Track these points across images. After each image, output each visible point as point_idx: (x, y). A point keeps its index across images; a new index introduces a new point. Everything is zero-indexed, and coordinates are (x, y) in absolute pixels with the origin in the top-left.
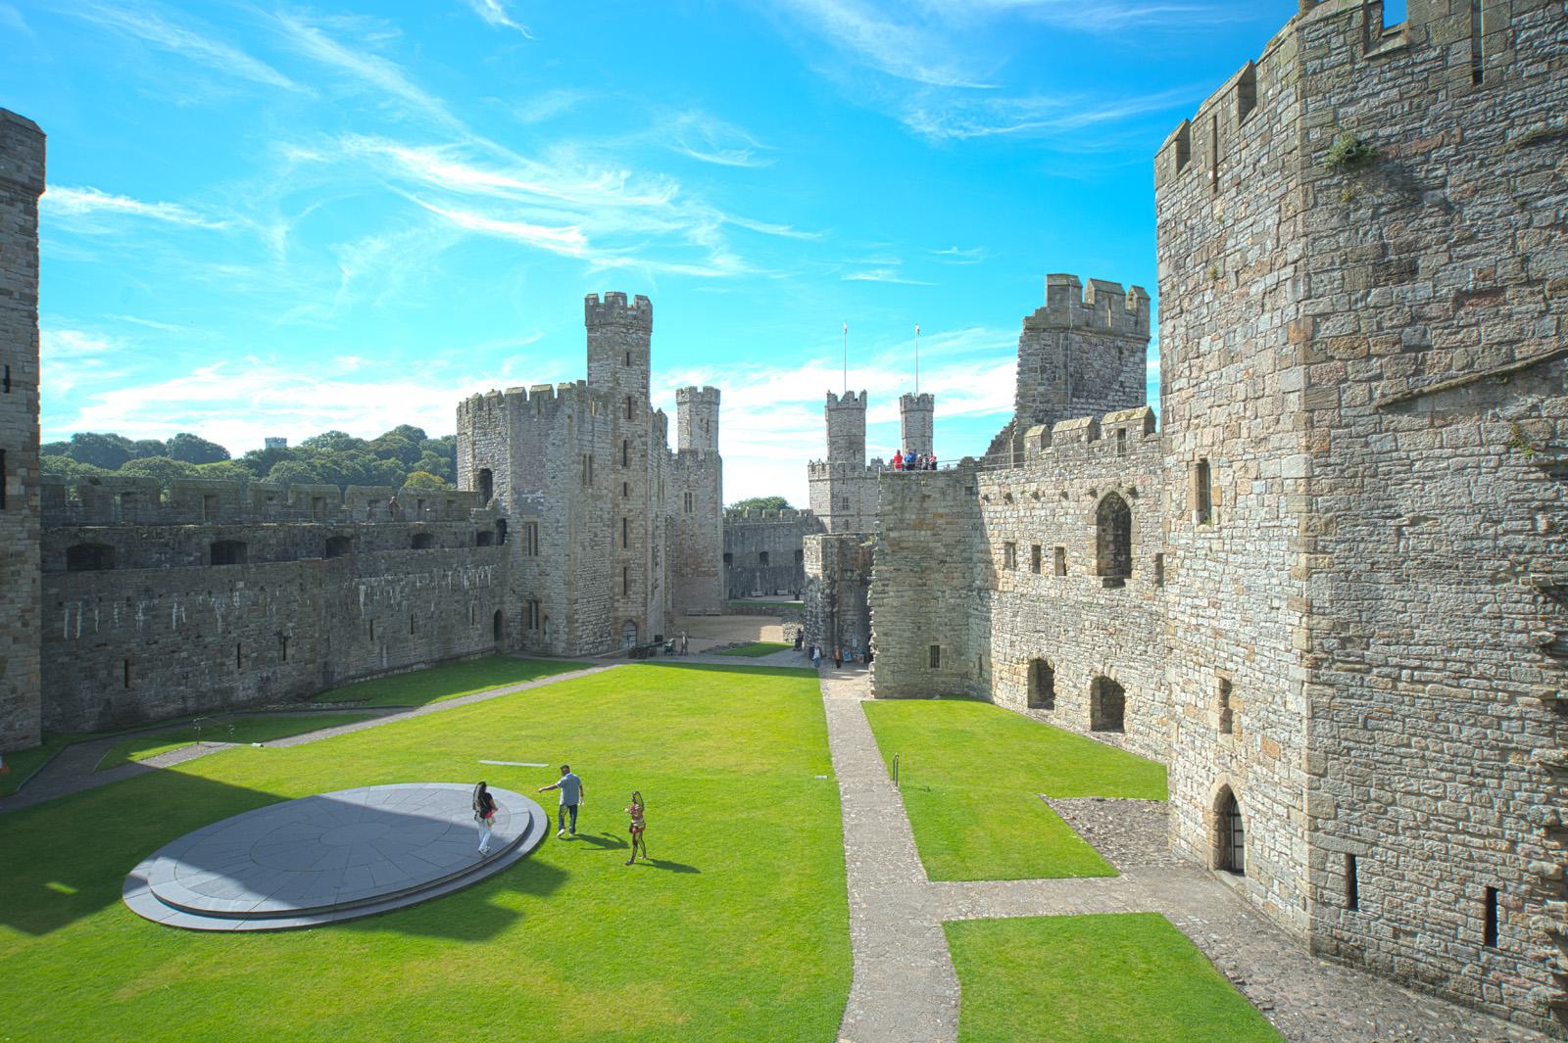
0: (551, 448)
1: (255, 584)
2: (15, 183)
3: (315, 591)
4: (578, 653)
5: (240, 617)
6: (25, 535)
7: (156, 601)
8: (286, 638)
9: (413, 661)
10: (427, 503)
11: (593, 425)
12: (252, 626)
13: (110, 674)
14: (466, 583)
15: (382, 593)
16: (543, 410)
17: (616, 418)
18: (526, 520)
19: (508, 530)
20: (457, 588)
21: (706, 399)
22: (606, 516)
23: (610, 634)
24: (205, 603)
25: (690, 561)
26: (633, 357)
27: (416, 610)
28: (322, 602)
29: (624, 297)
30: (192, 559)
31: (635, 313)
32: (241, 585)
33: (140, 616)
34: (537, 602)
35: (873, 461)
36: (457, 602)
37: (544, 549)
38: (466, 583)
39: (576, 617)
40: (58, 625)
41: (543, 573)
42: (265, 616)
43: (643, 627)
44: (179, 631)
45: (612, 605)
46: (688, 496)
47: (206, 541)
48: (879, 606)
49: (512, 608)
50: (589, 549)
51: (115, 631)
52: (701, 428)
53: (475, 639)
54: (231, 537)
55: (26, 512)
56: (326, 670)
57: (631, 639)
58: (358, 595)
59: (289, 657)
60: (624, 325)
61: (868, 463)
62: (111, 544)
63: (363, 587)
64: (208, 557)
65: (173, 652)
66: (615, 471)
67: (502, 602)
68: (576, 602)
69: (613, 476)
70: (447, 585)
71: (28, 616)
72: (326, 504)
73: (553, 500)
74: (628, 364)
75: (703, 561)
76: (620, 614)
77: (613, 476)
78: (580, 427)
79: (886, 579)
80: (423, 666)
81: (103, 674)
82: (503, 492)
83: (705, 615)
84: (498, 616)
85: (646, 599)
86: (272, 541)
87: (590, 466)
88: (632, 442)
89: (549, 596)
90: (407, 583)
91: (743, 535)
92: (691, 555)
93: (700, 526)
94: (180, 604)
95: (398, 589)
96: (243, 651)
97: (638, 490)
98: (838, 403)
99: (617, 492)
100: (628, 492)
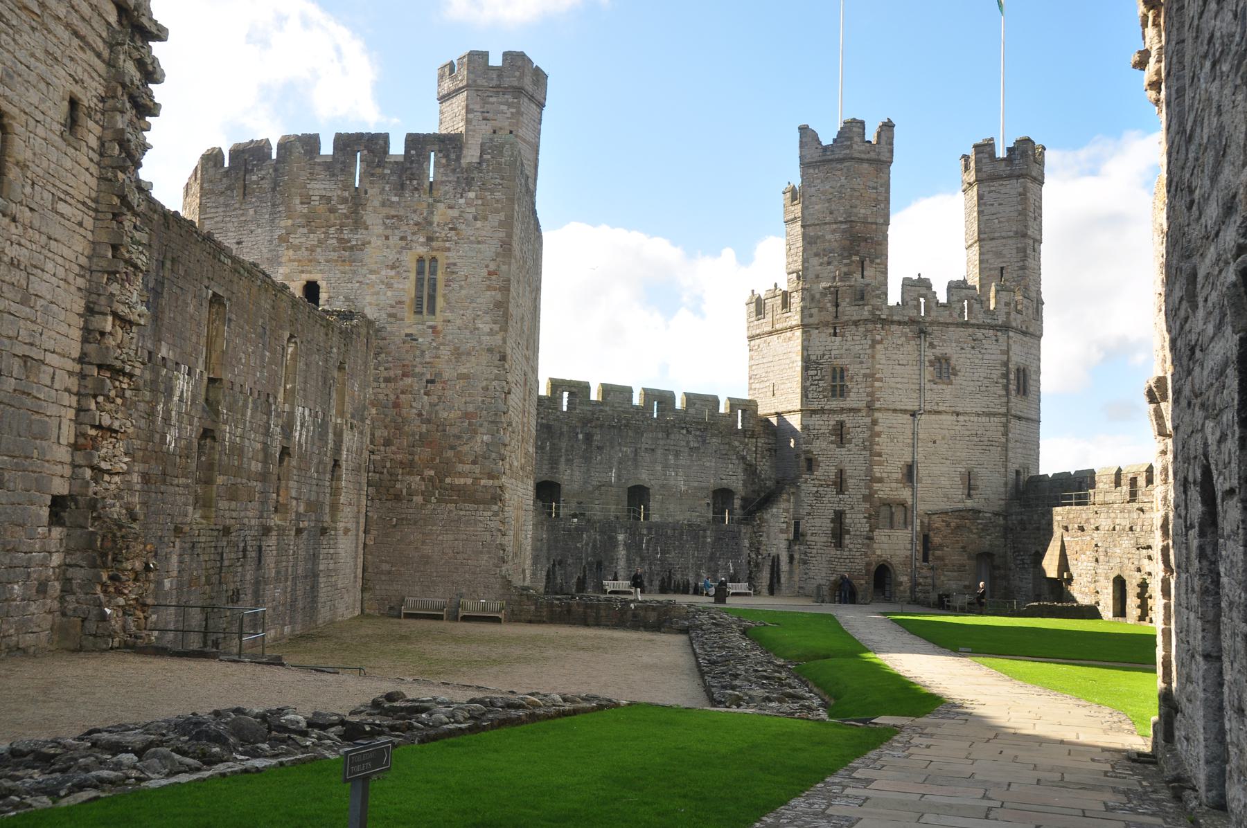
21: (507, 82)
25: (422, 454)
35: (907, 284)
61: (894, 296)
75: (458, 455)
83: (454, 618)
91: (588, 438)
92: (424, 440)
93: (458, 354)
98: (826, 148)
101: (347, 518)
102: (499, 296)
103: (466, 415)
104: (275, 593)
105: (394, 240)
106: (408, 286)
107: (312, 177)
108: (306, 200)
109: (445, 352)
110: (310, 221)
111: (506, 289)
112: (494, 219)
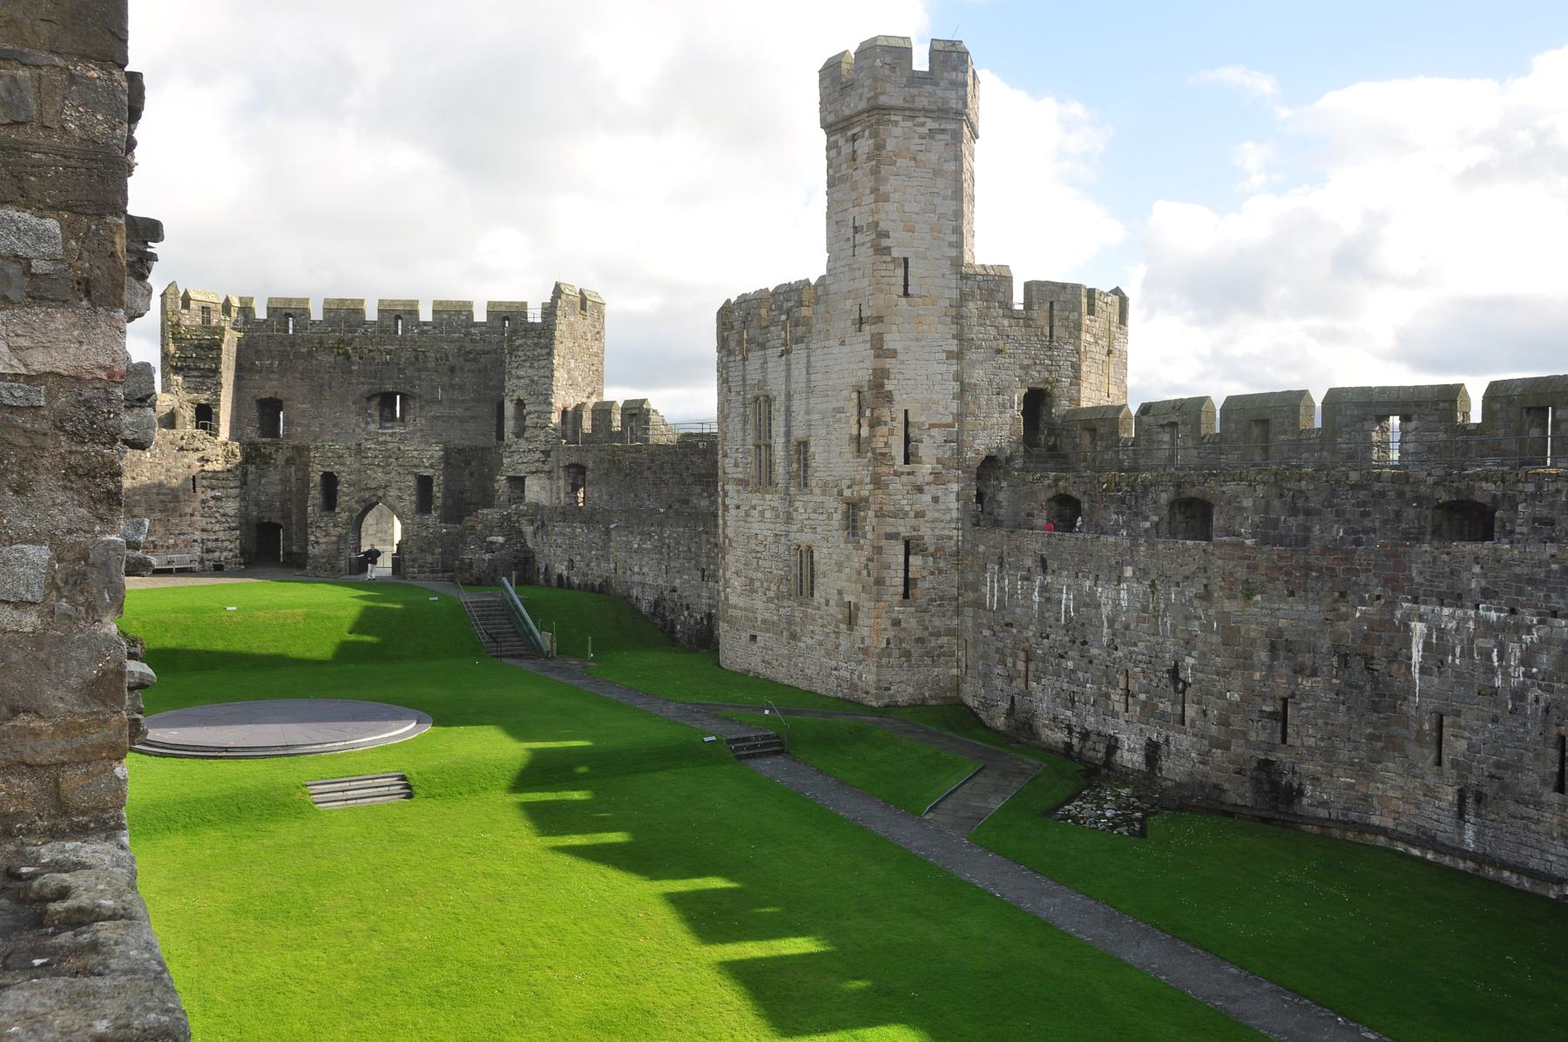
6: (868, 480)
7: (1049, 579)
15: (1467, 653)
24: (1092, 594)
30: (1148, 525)
32: (1128, 572)
33: (1036, 597)
44: (1067, 628)
47: (1164, 498)
51: (1018, 610)
58: (1409, 640)
63: (1418, 628)
64: (1164, 527)
65: (1061, 656)
71: (871, 565)
81: (1010, 660)
86: (1248, 503)
90: (1545, 642)
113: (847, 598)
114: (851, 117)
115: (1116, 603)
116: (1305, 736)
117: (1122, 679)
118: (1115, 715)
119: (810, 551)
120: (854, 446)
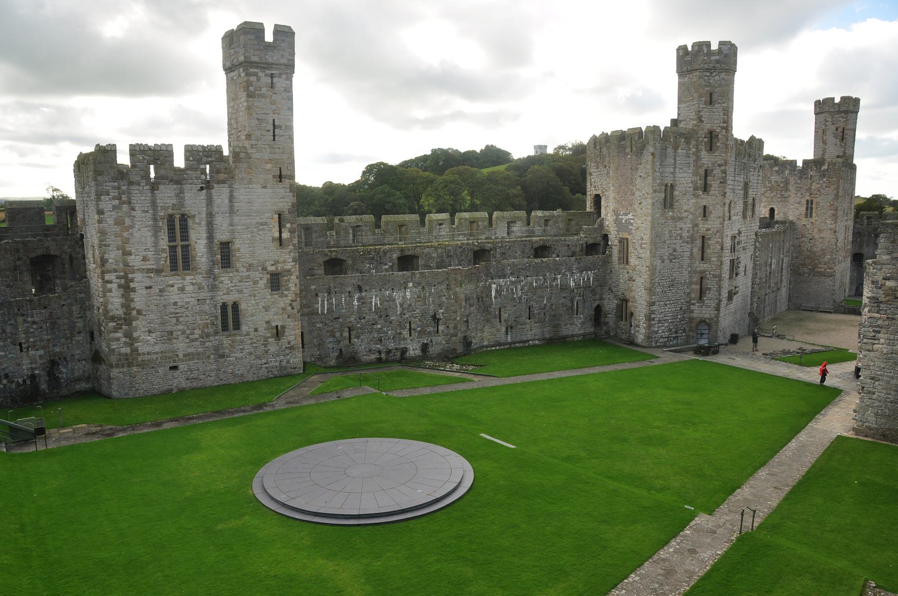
0: (639, 180)
1: (419, 284)
2: (281, 65)
3: (458, 289)
4: (654, 345)
5: (410, 305)
6: (291, 260)
7: (364, 294)
8: (439, 320)
9: (529, 338)
10: (551, 223)
11: (675, 159)
12: (418, 311)
13: (341, 335)
14: (572, 284)
15: (507, 290)
16: (634, 149)
17: (698, 151)
18: (621, 236)
19: (610, 243)
20: (564, 287)
22: (685, 234)
23: (684, 331)
25: (808, 261)
26: (715, 97)
27: (532, 303)
28: (462, 296)
29: (708, 44)
31: (718, 57)
32: (411, 285)
33: (356, 303)
34: (627, 301)
36: (564, 297)
37: (633, 260)
38: (572, 284)
39: (653, 316)
40: (316, 306)
41: (631, 279)
42: (425, 304)
43: (714, 327)
45: (689, 308)
46: (809, 203)
47: (395, 256)
48: (869, 351)
49: (610, 305)
50: (667, 262)
52: (836, 137)
53: (577, 326)
54: (409, 253)
55: (291, 247)
56: (467, 342)
57: (704, 336)
59: (440, 332)
60: (708, 70)
62: (345, 258)
63: (494, 286)
64: (396, 267)
66: (696, 196)
67: (601, 299)
68: (653, 304)
69: (694, 201)
70: (557, 285)
71: (294, 304)
72: (478, 226)
73: (639, 222)
74: (711, 103)
75: (820, 263)
76: (695, 315)
77: (694, 201)
78: (662, 162)
79: (878, 326)
80: (537, 342)
81: (338, 335)
82: (608, 215)
83: (817, 311)
84: (598, 309)
85: (719, 304)
86: (435, 255)
87: (672, 194)
88: (712, 170)
89: (634, 298)
92: (808, 257)
93: (820, 231)
94: (376, 296)
95: (519, 287)
96: (413, 326)
97: (716, 212)
99: (697, 213)
100: (707, 214)
101: (785, 283)
102: (833, 212)
103: (822, 250)
104: (767, 309)
105: (799, 195)
106: (804, 209)
107: (772, 175)
108: (770, 182)
109: (815, 230)
110: (771, 189)
111: (836, 210)
112: (833, 187)
113: (274, 324)
114: (273, 64)
115: (404, 297)
116: (472, 325)
117: (408, 325)
118: (405, 339)
119: (235, 306)
120: (278, 243)
